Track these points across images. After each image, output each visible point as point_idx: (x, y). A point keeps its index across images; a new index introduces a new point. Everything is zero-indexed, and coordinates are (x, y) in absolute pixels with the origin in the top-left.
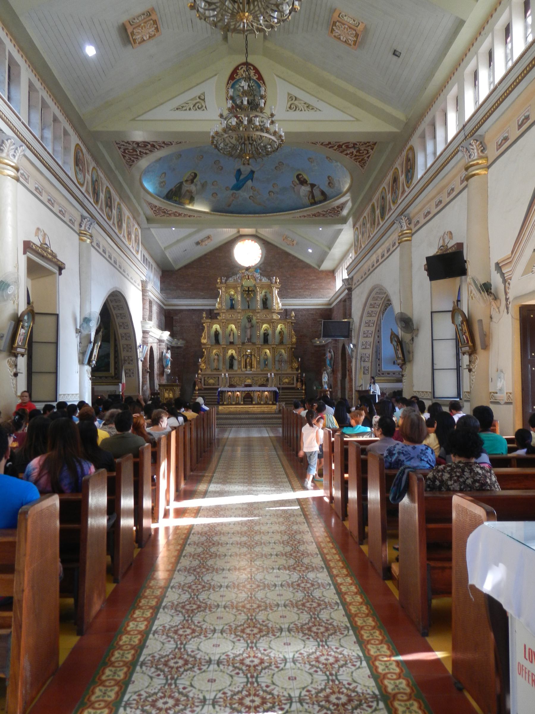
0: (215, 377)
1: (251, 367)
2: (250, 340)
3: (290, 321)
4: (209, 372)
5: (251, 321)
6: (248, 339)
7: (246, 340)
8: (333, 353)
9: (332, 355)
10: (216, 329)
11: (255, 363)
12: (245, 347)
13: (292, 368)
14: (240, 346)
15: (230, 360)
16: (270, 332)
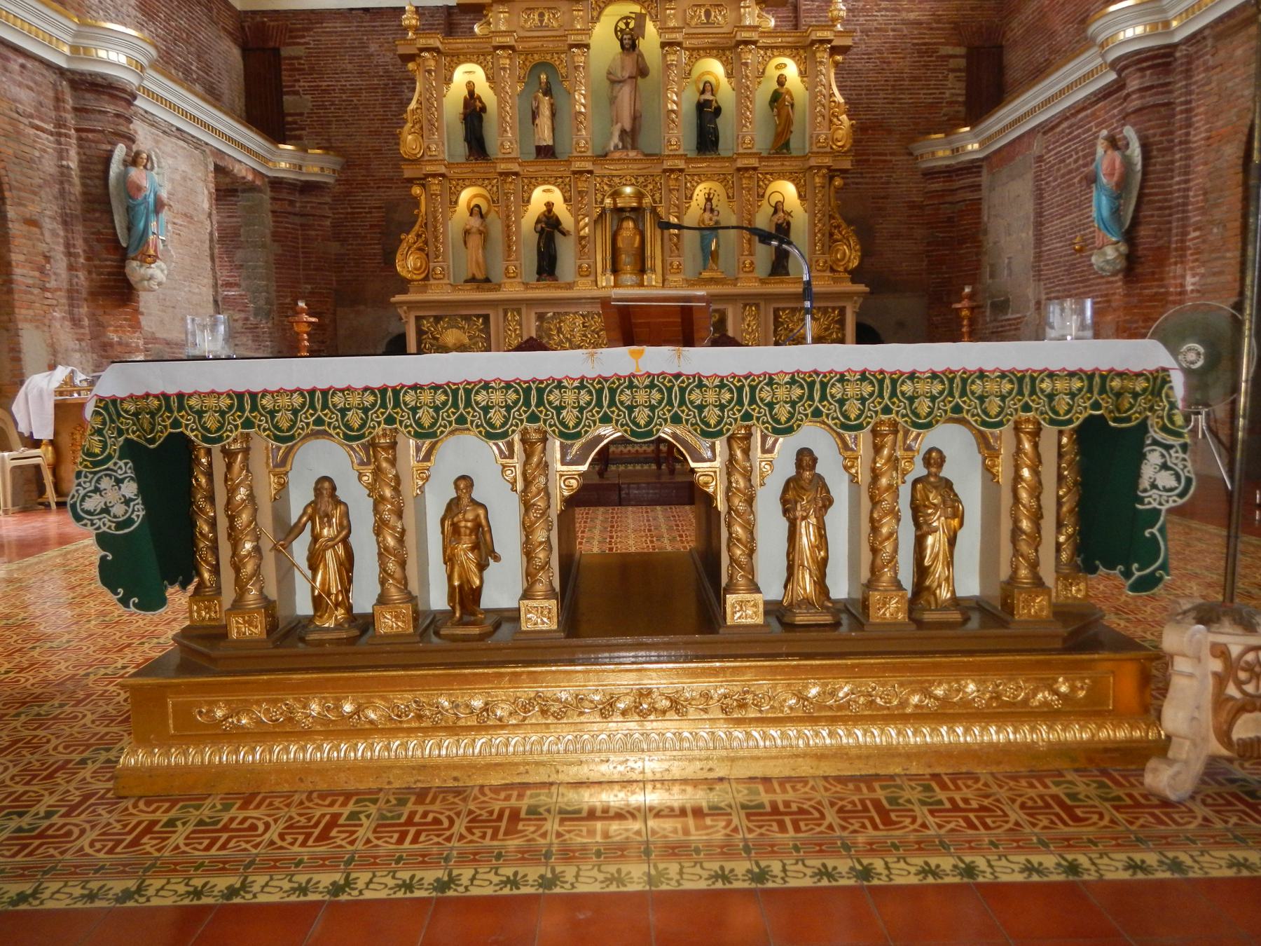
0: (467, 318)
1: (642, 271)
2: (630, 137)
3: (827, 35)
4: (438, 293)
5: (634, 46)
6: (623, 132)
7: (616, 140)
8: (1135, 151)
9: (1127, 163)
10: (470, 87)
11: (655, 251)
12: (610, 169)
13: (832, 270)
14: (588, 166)
15: (541, 232)
16: (726, 93)
